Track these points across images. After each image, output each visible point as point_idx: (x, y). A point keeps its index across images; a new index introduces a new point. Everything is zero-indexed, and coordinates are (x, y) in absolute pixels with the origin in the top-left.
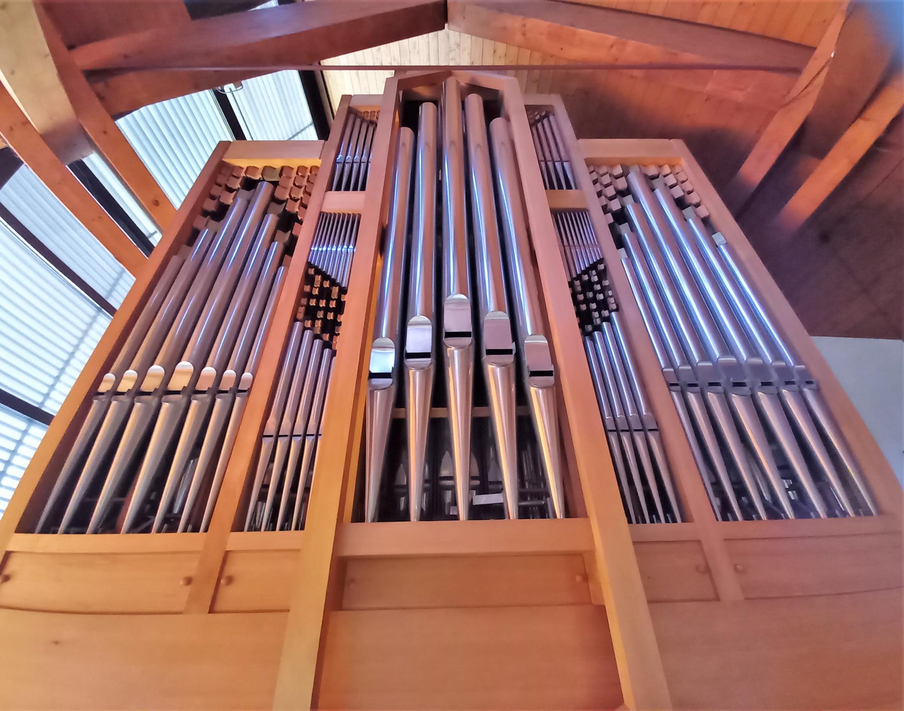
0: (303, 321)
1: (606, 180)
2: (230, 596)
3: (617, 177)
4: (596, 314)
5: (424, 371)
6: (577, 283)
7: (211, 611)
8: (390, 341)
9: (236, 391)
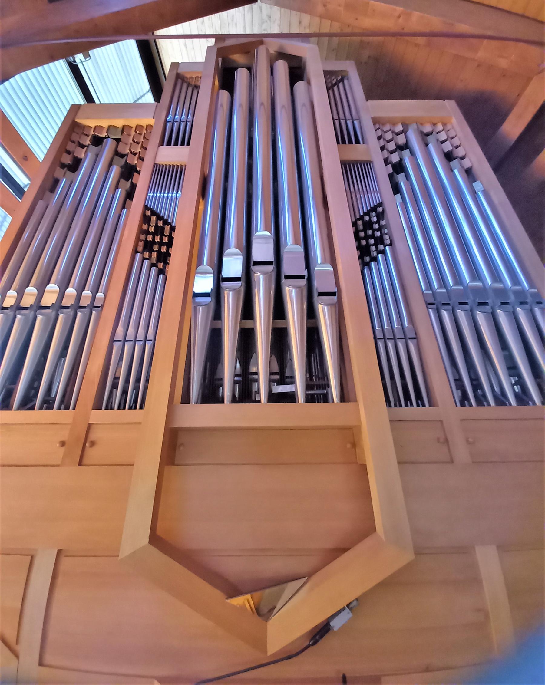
0: (142, 253)
1: (389, 136)
2: (92, 454)
3: (398, 134)
4: (373, 248)
5: (236, 291)
6: (360, 223)
7: (80, 465)
8: (210, 269)
9: (93, 306)
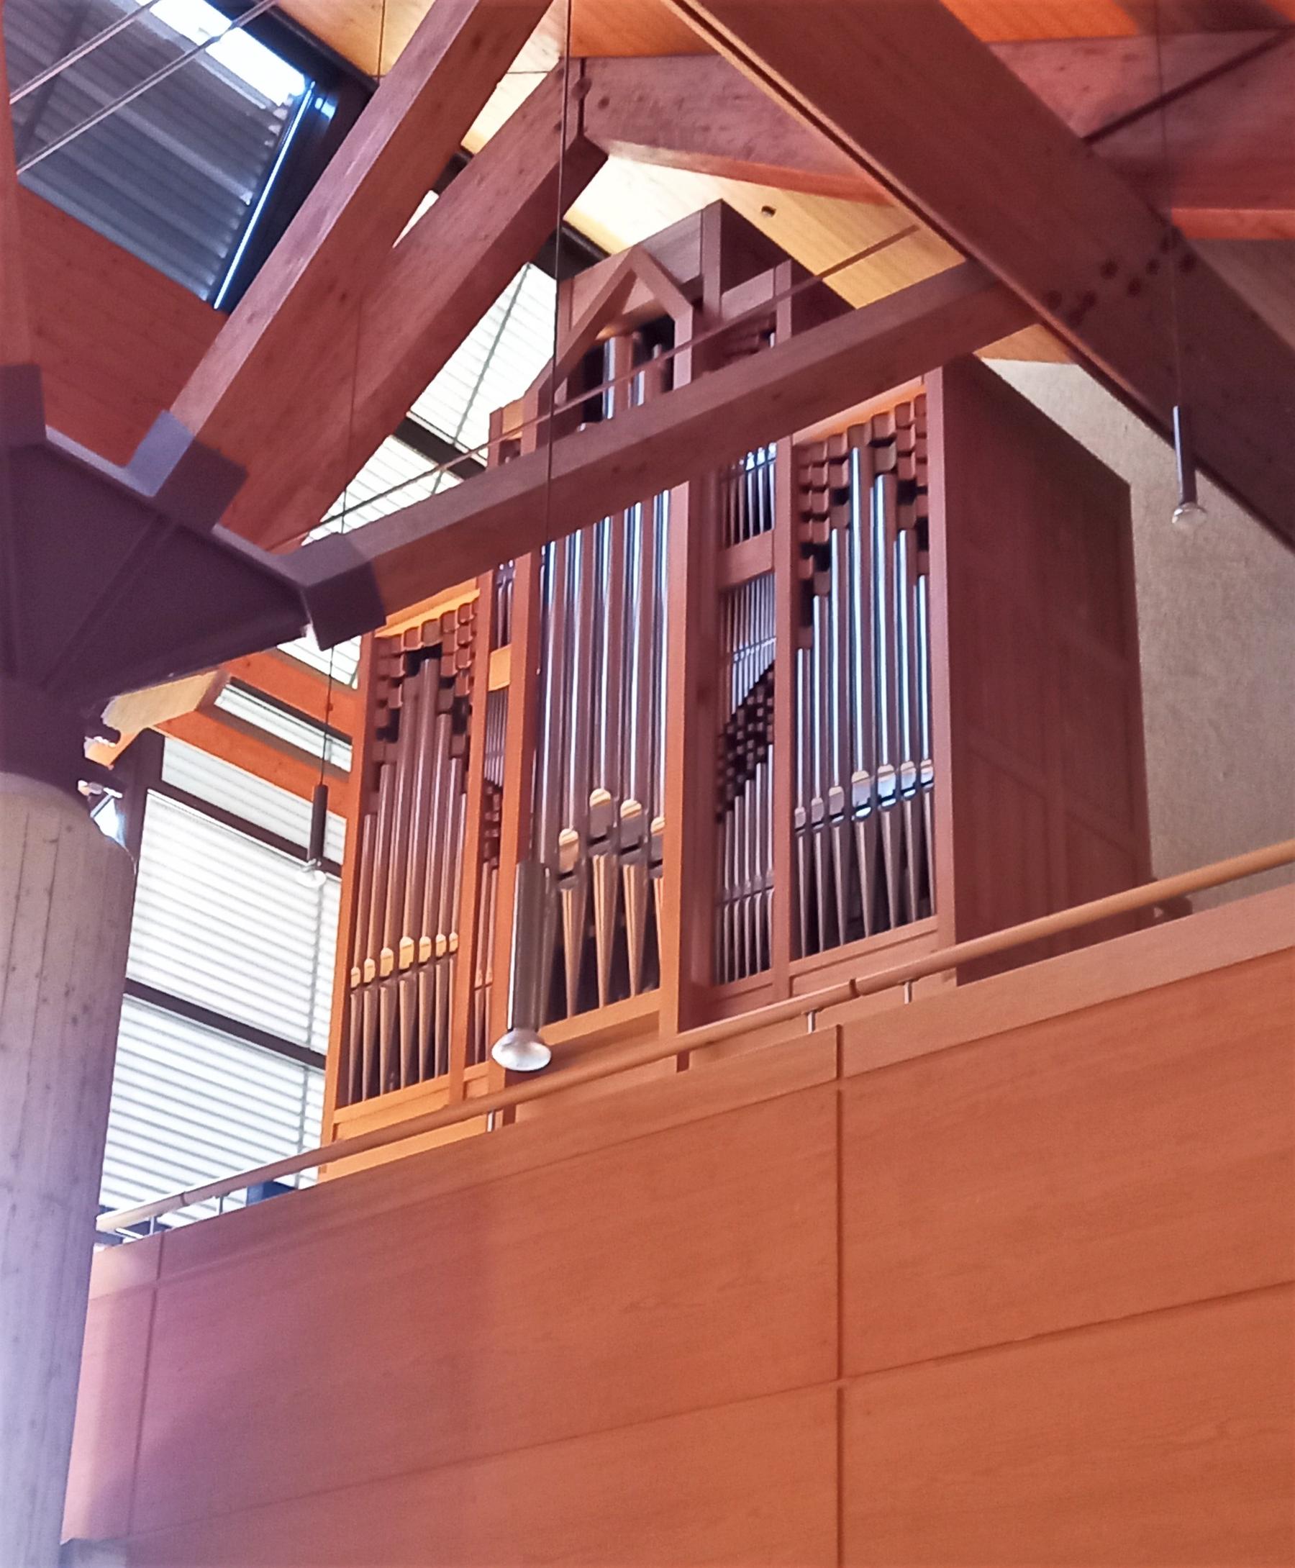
9: (448, 954)
